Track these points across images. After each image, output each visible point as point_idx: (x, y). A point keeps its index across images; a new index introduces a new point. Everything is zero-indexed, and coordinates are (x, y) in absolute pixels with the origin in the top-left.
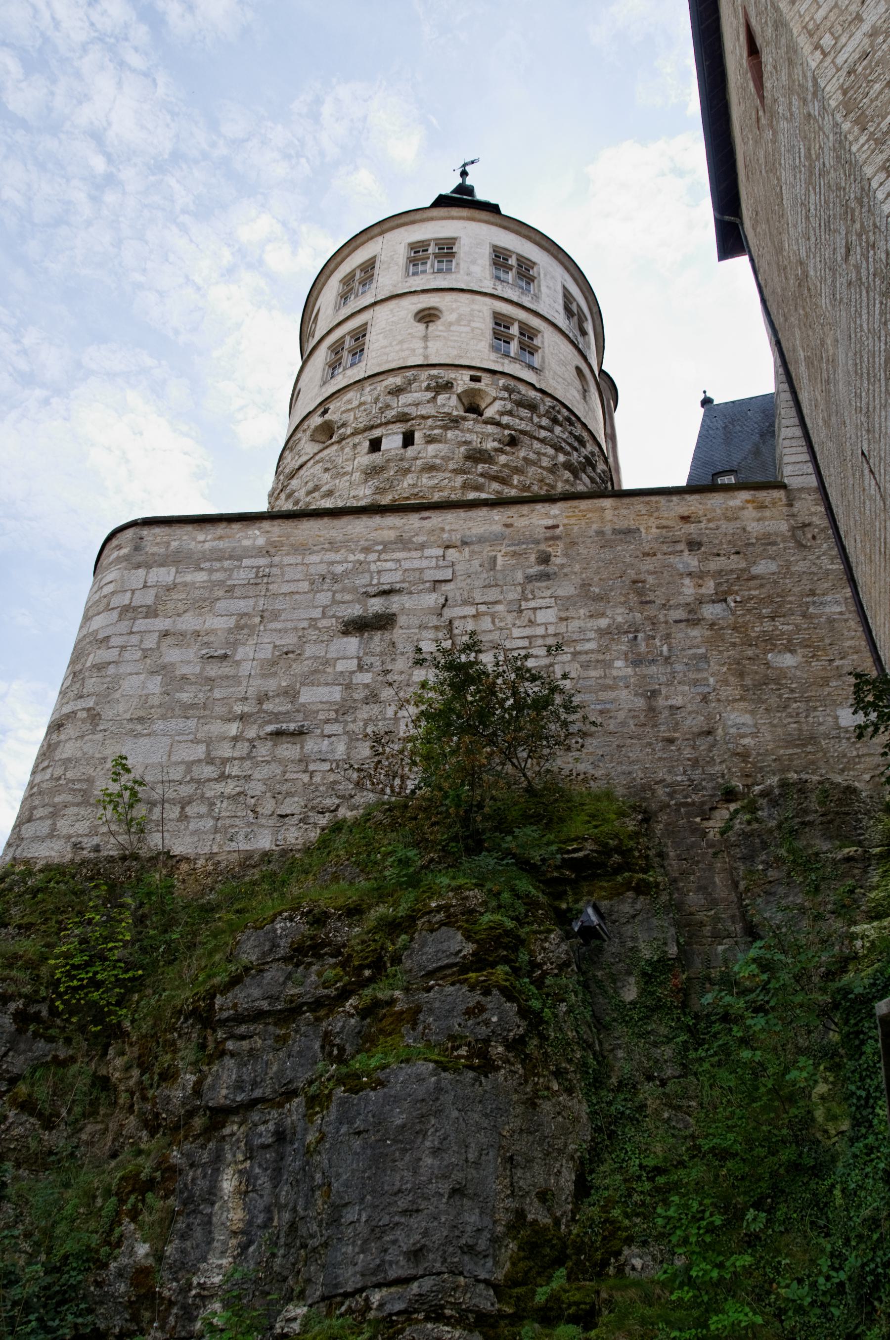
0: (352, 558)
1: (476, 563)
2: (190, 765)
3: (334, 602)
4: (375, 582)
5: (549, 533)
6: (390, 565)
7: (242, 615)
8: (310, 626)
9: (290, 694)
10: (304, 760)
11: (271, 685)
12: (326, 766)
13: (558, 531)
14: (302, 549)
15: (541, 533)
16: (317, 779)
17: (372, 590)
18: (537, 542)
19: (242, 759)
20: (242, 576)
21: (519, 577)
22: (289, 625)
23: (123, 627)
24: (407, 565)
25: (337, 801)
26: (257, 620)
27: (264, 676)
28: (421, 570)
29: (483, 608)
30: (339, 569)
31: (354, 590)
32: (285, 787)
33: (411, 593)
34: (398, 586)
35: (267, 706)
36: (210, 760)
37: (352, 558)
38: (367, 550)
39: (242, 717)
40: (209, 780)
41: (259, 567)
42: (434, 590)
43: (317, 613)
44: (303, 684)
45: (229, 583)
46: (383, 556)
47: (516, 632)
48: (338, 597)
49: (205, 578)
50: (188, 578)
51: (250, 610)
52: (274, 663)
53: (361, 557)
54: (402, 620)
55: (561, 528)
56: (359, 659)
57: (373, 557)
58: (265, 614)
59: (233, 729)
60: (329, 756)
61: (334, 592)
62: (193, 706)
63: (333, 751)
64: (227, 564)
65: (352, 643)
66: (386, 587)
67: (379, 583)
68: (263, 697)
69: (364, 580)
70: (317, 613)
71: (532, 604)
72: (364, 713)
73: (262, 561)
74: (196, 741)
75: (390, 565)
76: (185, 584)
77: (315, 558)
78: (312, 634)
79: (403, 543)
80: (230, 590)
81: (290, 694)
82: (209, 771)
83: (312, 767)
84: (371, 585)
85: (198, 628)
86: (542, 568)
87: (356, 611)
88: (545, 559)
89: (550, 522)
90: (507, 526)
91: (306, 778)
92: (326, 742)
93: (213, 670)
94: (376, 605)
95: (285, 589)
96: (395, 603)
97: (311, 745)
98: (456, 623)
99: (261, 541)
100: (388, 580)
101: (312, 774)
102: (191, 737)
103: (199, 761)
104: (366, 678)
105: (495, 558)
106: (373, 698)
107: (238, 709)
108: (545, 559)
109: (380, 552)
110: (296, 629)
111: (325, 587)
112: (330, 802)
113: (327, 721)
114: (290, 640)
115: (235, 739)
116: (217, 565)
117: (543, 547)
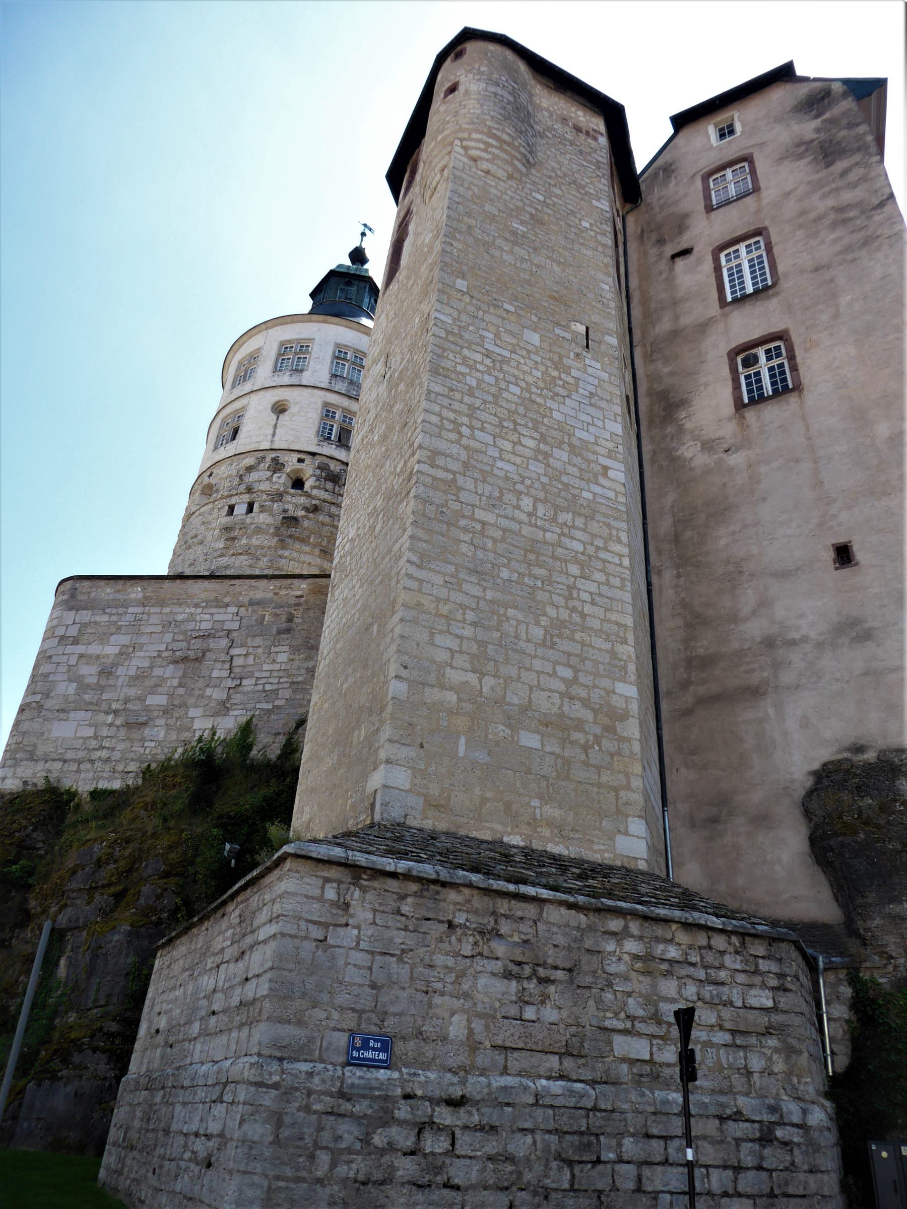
0: (187, 611)
1: (254, 618)
3: (174, 640)
5: (297, 601)
6: (207, 617)
7: (123, 646)
8: (159, 656)
9: (141, 698)
11: (132, 692)
14: (162, 603)
15: (293, 601)
17: (195, 634)
21: (274, 631)
24: (216, 618)
26: (131, 649)
29: (251, 650)
30: (180, 618)
33: (214, 637)
35: (129, 706)
37: (187, 611)
43: (163, 648)
45: (119, 623)
46: (205, 611)
47: (266, 667)
49: (107, 619)
50: (98, 619)
51: (128, 643)
53: (193, 610)
57: (199, 610)
61: (175, 634)
62: (91, 703)
64: (121, 610)
68: (127, 701)
69: (191, 626)
70: (163, 648)
73: (140, 610)
74: (90, 725)
76: (96, 622)
78: (159, 661)
80: (120, 627)
81: (141, 698)
88: (290, 619)
90: (276, 594)
102: (87, 723)
103: (90, 737)
105: (263, 617)
107: (114, 706)
108: (290, 619)
109: (203, 608)
115: (110, 725)
116: (114, 611)
117: (292, 610)
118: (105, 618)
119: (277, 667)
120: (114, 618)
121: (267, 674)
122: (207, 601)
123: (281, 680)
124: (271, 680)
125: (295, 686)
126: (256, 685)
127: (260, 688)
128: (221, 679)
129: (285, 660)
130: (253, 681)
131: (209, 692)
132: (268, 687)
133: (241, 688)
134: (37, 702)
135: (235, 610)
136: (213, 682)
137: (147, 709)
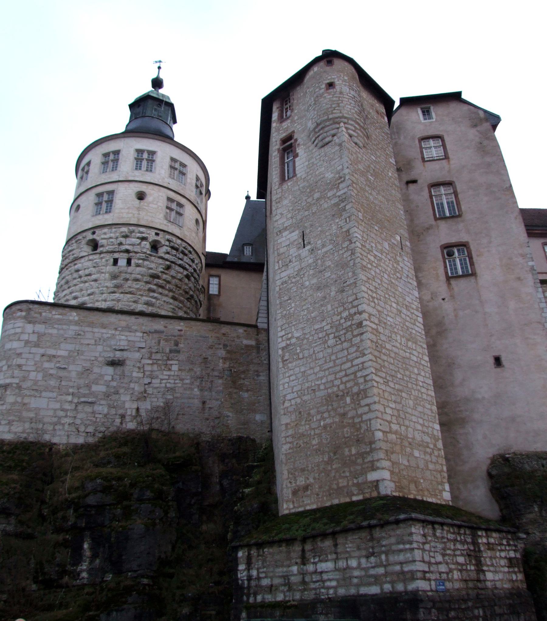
0: (110, 332)
2: (55, 410)
4: (118, 344)
5: (179, 333)
6: (123, 337)
7: (70, 351)
8: (95, 360)
10: (93, 412)
11: (82, 382)
12: (101, 416)
13: (182, 333)
14: (91, 325)
16: (98, 420)
17: (117, 348)
18: (175, 336)
19: (73, 410)
20: (71, 333)
22: (88, 358)
23: (27, 350)
24: (130, 339)
25: (105, 429)
26: (76, 354)
27: (80, 378)
28: (134, 342)
29: (155, 361)
30: (105, 336)
31: (110, 346)
32: (88, 422)
33: (130, 351)
34: (126, 348)
35: (81, 390)
36: (62, 410)
37: (110, 332)
38: (116, 329)
39: (73, 394)
40: (62, 417)
41: (76, 330)
42: (139, 351)
43: (97, 354)
44: (93, 383)
45: (66, 336)
46: (122, 333)
47: (165, 373)
48: (105, 348)
50: (51, 331)
51: (73, 349)
52: (83, 374)
53: (113, 332)
54: (128, 362)
55: (183, 332)
56: (112, 376)
57: (118, 333)
58: (79, 352)
59: (70, 398)
60: (102, 412)
62: (55, 387)
63: (103, 411)
64: (65, 327)
65: (110, 370)
66: (122, 348)
67: (120, 345)
71: (171, 362)
72: (114, 397)
73: (77, 328)
74: (57, 402)
75: (123, 337)
76: (49, 334)
77: (96, 330)
78: (96, 363)
79: (128, 328)
81: (88, 386)
82: (62, 413)
83: (97, 416)
84: (116, 345)
85: (54, 354)
86: (175, 347)
87: (110, 355)
89: (180, 328)
91: (94, 419)
92: (101, 407)
93: (62, 373)
94: (118, 354)
95: (86, 342)
96: (125, 354)
97: (97, 408)
98: (145, 366)
99: (76, 318)
100: (123, 344)
101: (96, 418)
103: (58, 409)
104: (114, 384)
106: (117, 393)
107: (71, 390)
108: (177, 344)
110: (90, 360)
111: (101, 343)
112: (103, 429)
113: (101, 399)
114: (87, 365)
116: (60, 327)
118: (54, 331)
119: (172, 373)
120: (61, 332)
121: (167, 377)
122: (122, 328)
123: (177, 382)
124: (169, 381)
125: (185, 386)
126: (161, 383)
127: (163, 385)
128: (139, 378)
129: (177, 369)
130: (158, 381)
131: (132, 385)
132: (168, 385)
133: (151, 385)
134: (17, 384)
135: (141, 335)
136: (135, 379)
137: (92, 394)
